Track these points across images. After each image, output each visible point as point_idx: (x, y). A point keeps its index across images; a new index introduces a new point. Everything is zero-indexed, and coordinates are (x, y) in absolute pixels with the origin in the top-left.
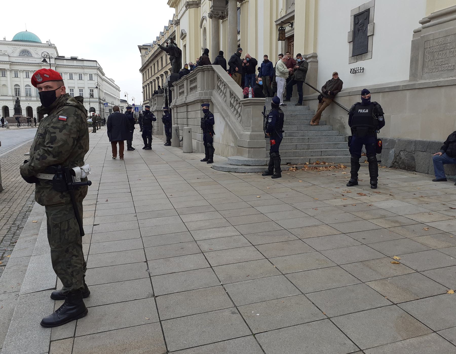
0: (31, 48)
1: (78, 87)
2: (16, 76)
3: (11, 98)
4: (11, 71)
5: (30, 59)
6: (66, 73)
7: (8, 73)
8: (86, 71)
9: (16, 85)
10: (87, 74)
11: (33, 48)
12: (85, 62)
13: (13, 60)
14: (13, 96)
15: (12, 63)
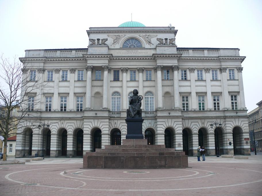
0: (141, 34)
1: (212, 93)
2: (116, 79)
3: (106, 114)
4: (109, 70)
5: (139, 51)
6: (192, 70)
7: (106, 73)
8: (224, 64)
9: (116, 93)
10: (225, 69)
11: (144, 34)
12: (221, 51)
13: (115, 53)
14: (109, 111)
15: (111, 58)
